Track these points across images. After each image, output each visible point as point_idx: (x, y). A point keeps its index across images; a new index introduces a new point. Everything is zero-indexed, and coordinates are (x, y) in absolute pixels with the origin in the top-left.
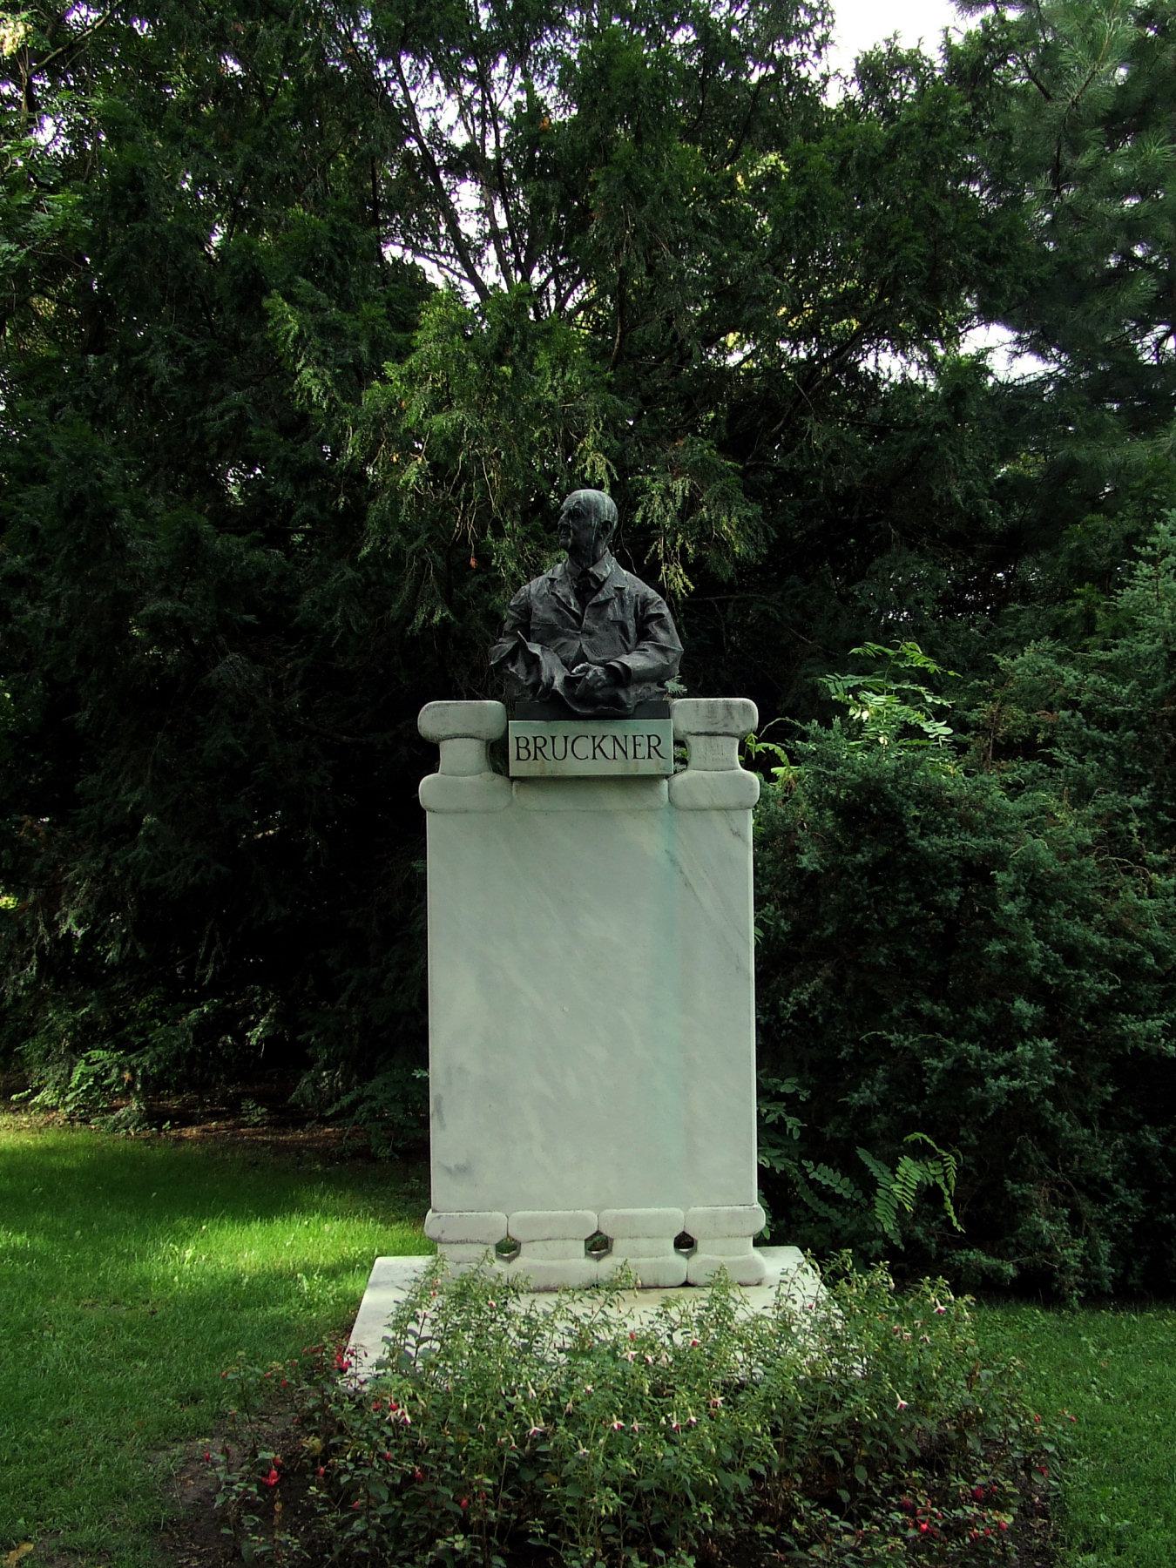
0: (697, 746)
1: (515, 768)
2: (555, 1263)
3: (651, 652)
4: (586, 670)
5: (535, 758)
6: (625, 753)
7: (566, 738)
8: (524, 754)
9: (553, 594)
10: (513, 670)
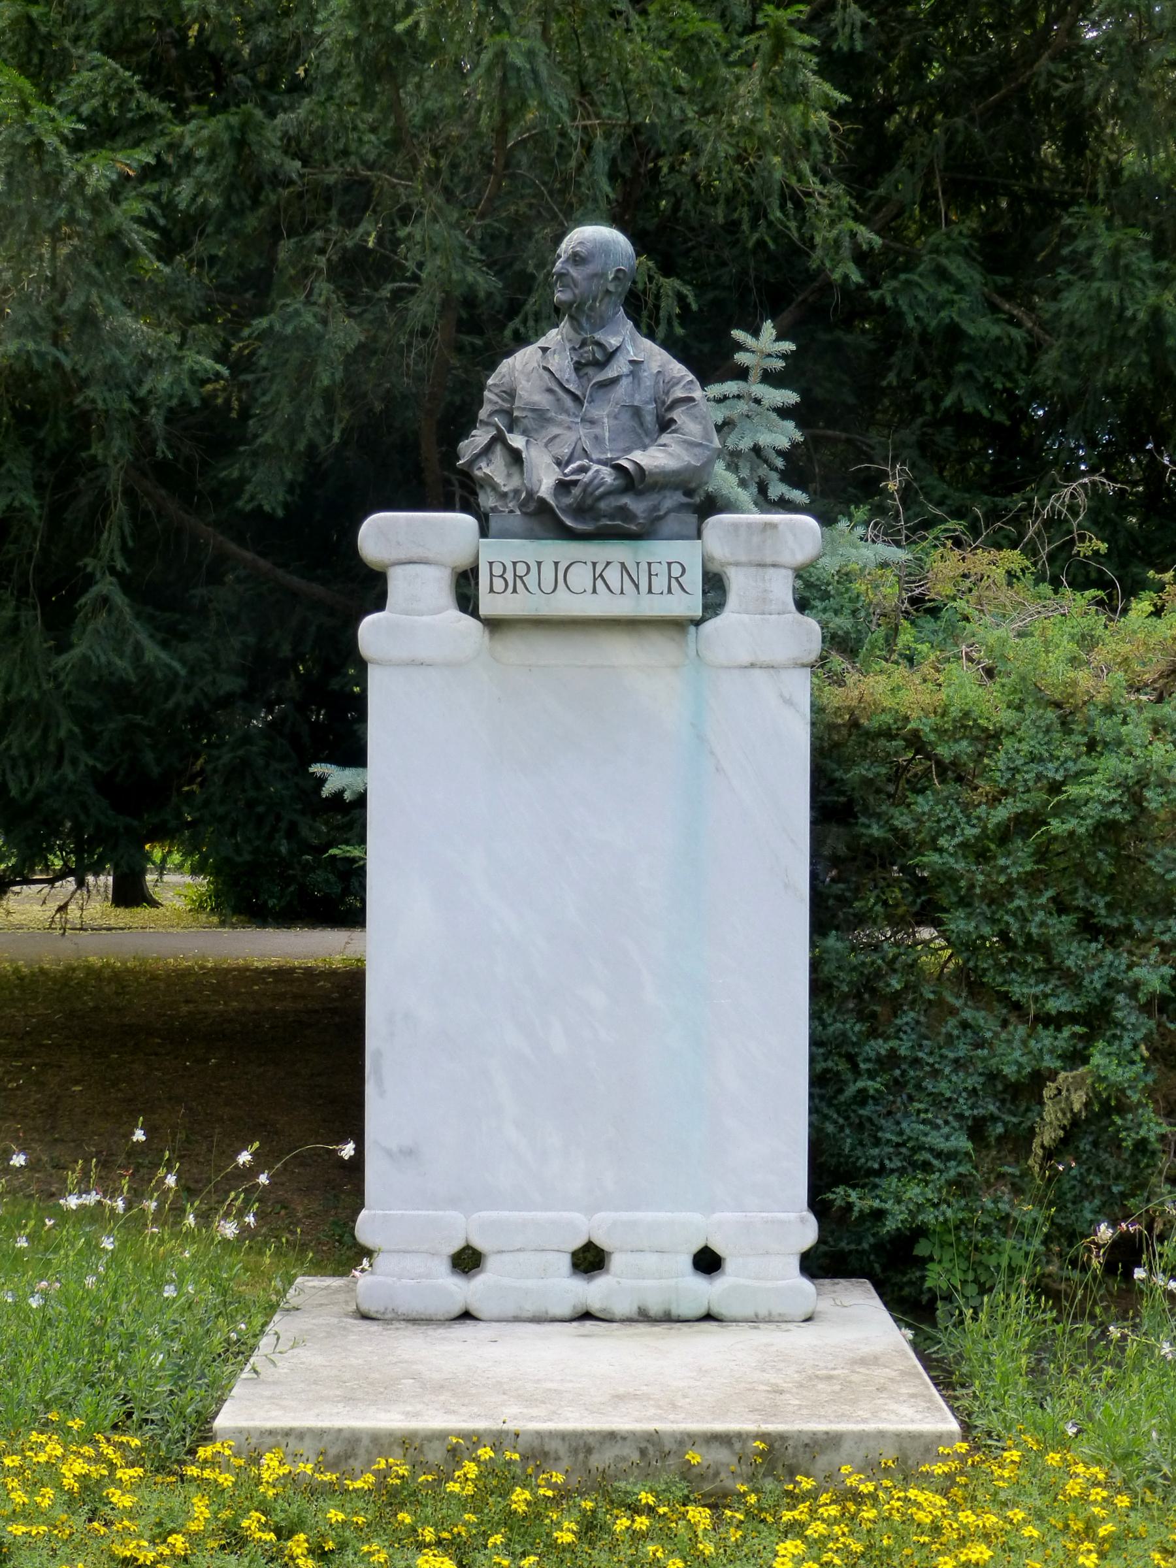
0: (738, 582)
1: (489, 605)
2: (531, 1283)
3: (675, 448)
4: (583, 469)
5: (515, 591)
6: (637, 586)
7: (556, 564)
8: (499, 584)
9: (546, 369)
10: (487, 471)
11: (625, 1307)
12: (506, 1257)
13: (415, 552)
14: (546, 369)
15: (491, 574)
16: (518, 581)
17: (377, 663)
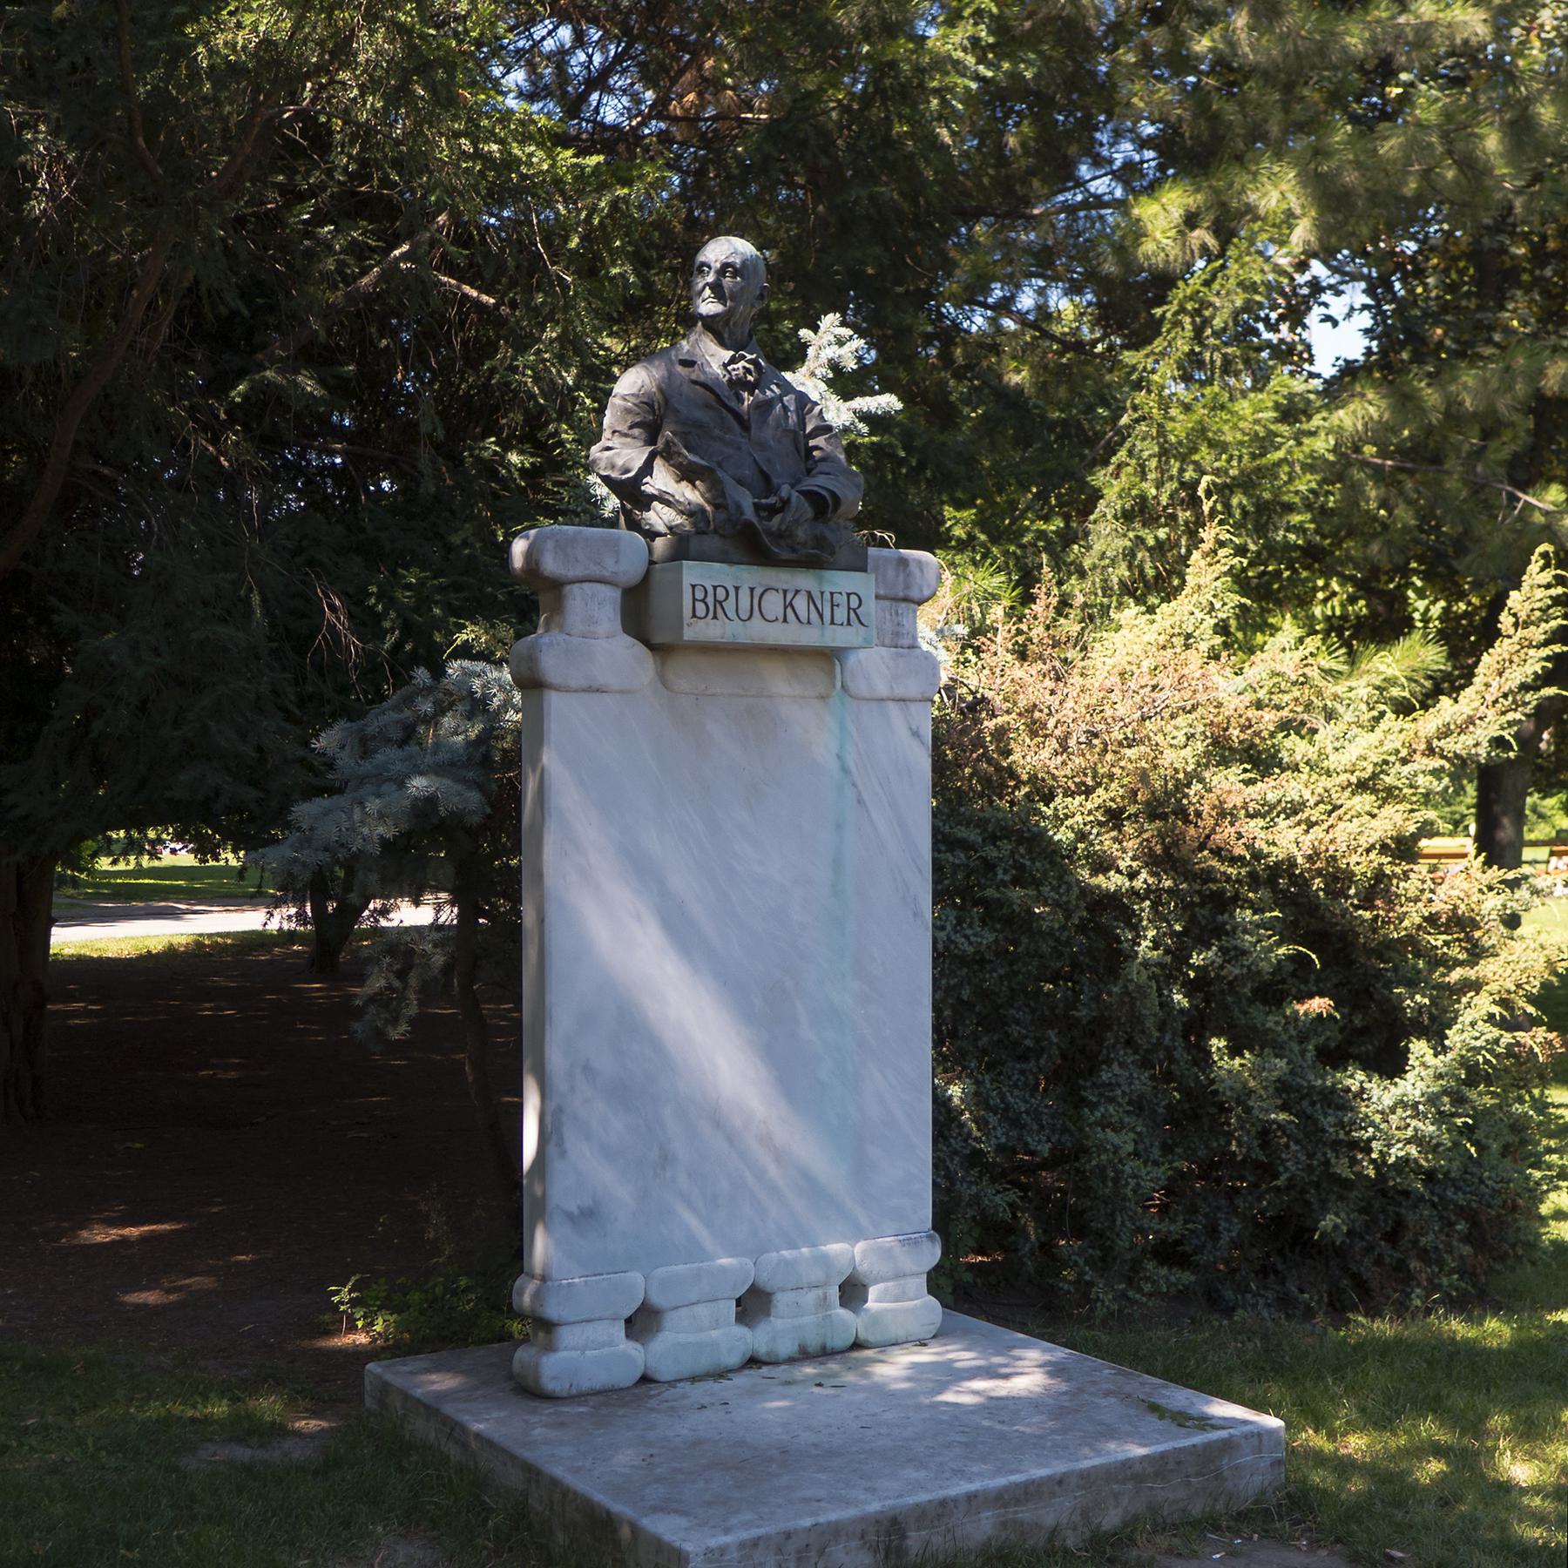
5: (715, 617)
6: (821, 616)
7: (752, 590)
8: (700, 608)
11: (786, 1348)
12: (683, 1312)
13: (595, 570)
15: (694, 600)
17: (557, 689)
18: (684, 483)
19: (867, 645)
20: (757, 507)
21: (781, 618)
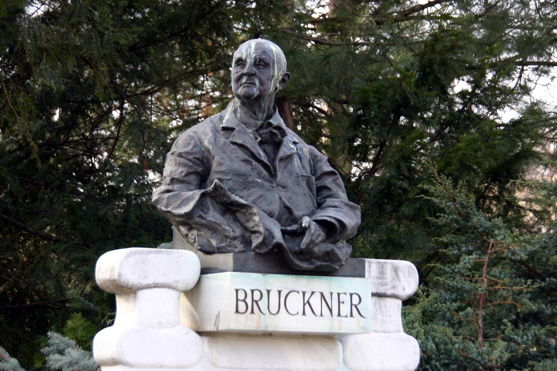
5: (252, 312)
6: (331, 311)
7: (280, 292)
9: (234, 143)
14: (234, 143)
15: (237, 300)
16: (254, 303)
18: (228, 216)
19: (365, 330)
20: (284, 232)
21: (301, 312)
